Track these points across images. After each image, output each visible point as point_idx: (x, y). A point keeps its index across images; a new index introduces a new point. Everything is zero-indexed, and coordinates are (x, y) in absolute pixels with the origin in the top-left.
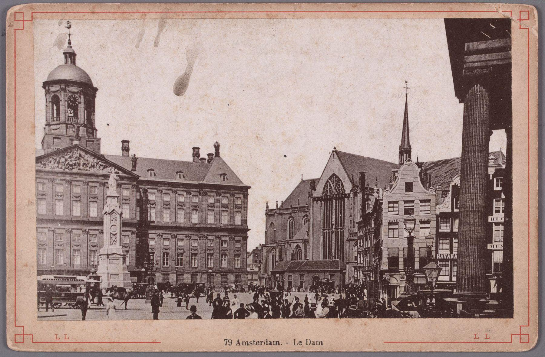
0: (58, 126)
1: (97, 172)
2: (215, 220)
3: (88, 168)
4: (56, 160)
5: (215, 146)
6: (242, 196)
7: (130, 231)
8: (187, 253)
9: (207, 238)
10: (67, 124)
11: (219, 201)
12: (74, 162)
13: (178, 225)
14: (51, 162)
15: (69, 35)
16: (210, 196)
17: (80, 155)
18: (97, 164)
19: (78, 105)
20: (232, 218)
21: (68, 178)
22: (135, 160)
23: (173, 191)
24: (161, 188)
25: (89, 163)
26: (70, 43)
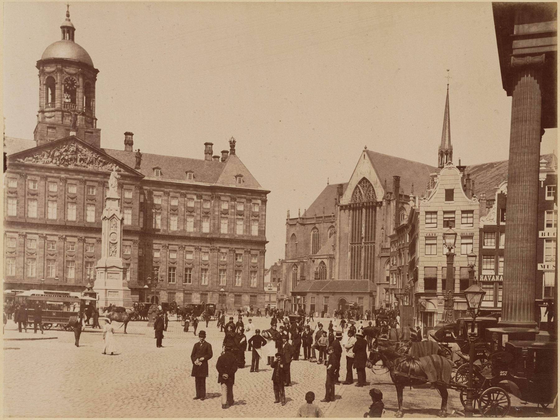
0: (53, 113)
2: (229, 229)
3: (85, 164)
4: (50, 153)
5: (230, 142)
6: (259, 202)
7: (131, 240)
8: (197, 268)
9: (219, 250)
10: (63, 112)
11: (234, 206)
12: (70, 156)
13: (187, 235)
14: (44, 156)
16: (224, 201)
17: (77, 149)
18: (96, 159)
19: (75, 90)
20: (248, 228)
22: (139, 156)
24: (168, 190)
25: (87, 158)
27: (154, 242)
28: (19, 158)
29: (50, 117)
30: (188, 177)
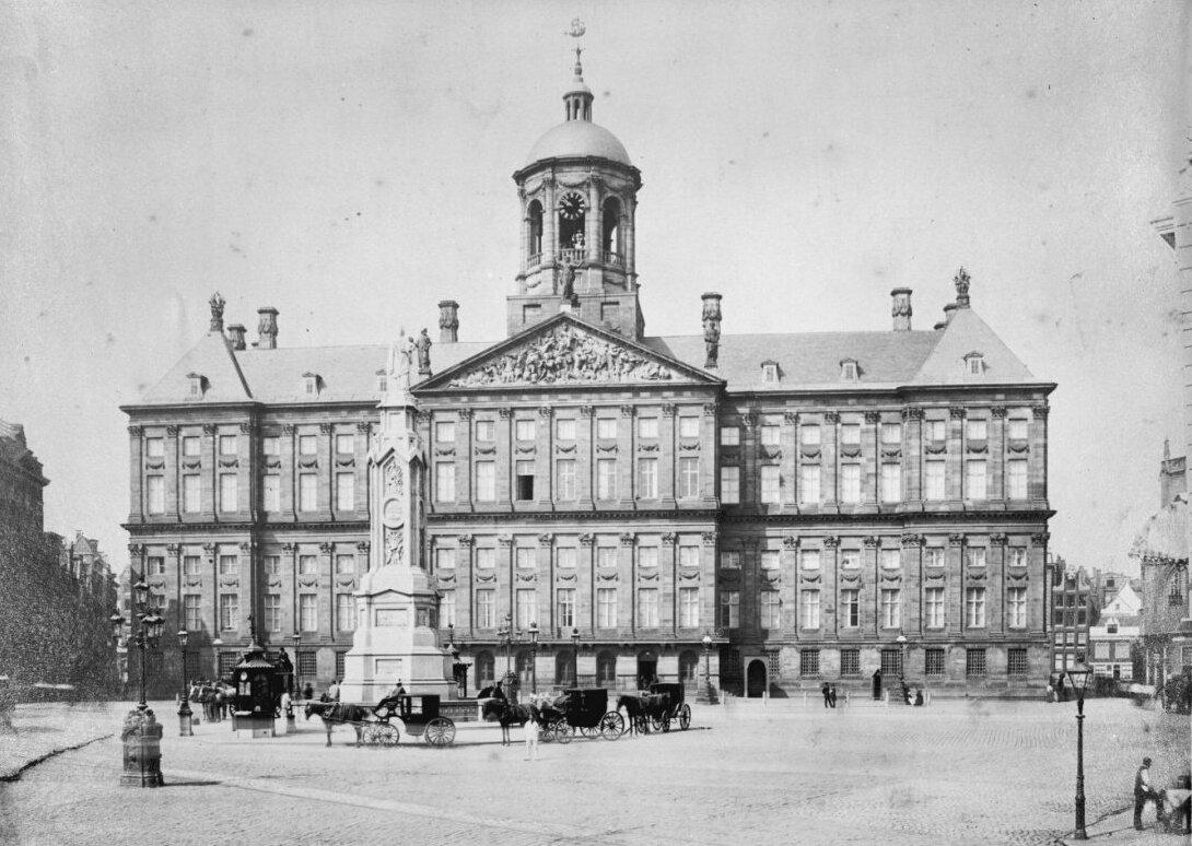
1: (615, 381)
3: (591, 373)
4: (516, 358)
7: (699, 533)
12: (558, 360)
15: (579, 52)
16: (933, 421)
19: (583, 216)
21: (546, 401)
23: (828, 416)
24: (794, 411)
25: (595, 359)
26: (579, 72)
27: (768, 534)
28: (457, 378)
29: (534, 286)
30: (844, 374)
